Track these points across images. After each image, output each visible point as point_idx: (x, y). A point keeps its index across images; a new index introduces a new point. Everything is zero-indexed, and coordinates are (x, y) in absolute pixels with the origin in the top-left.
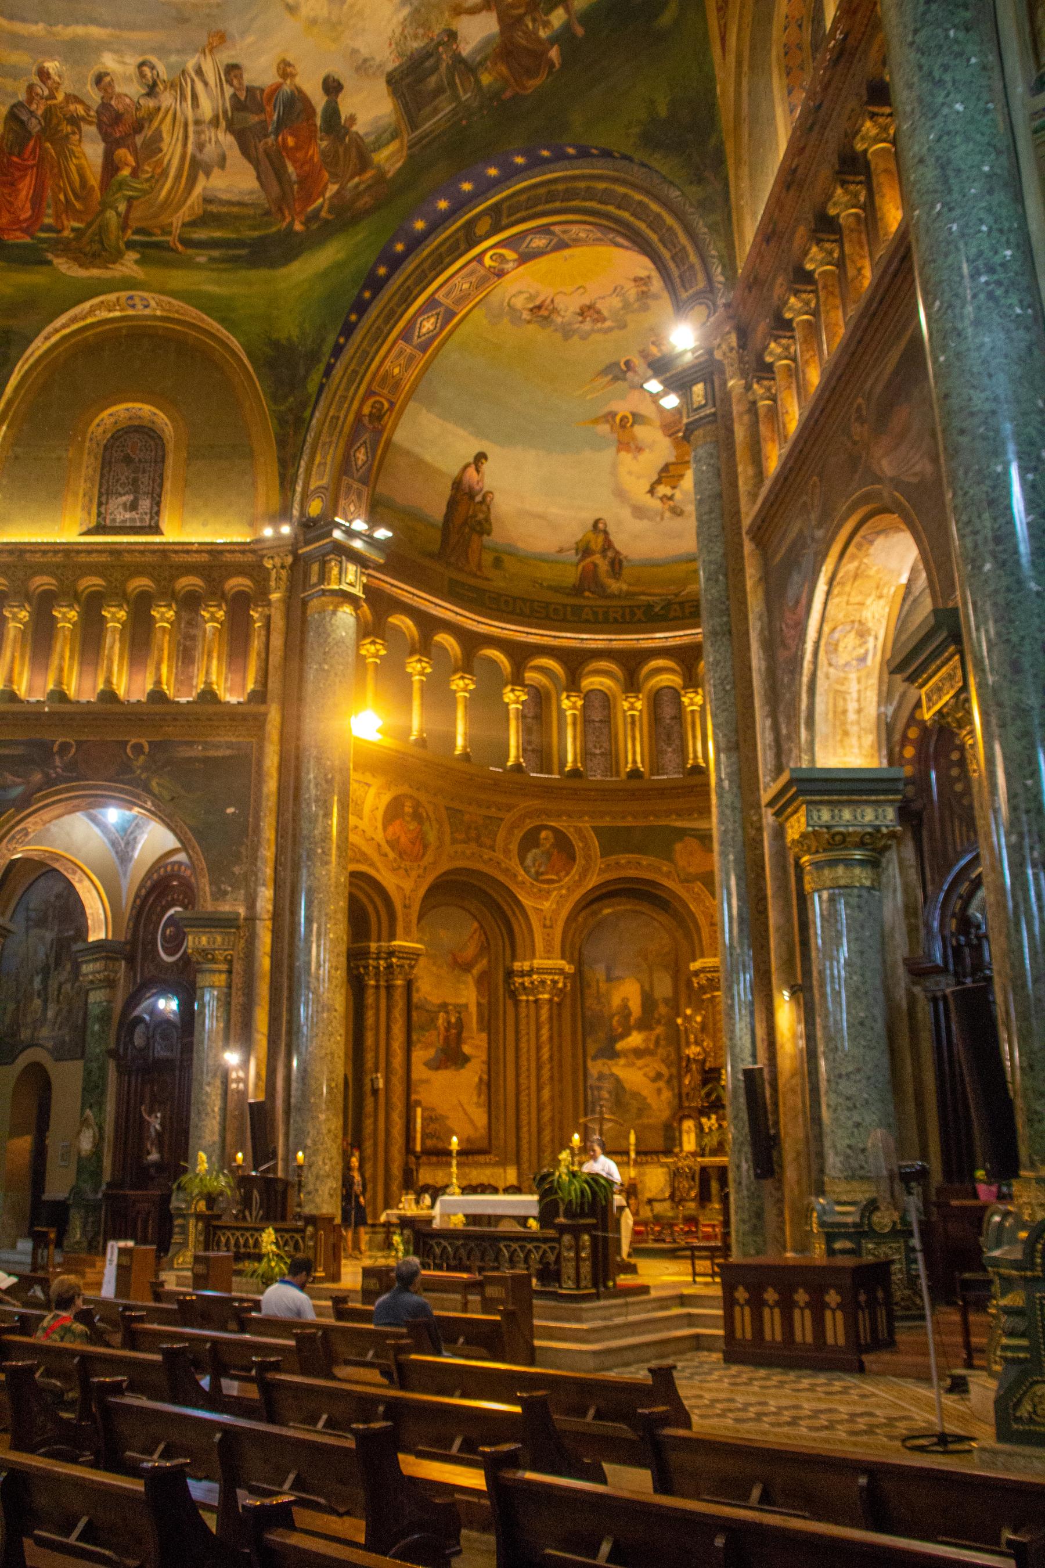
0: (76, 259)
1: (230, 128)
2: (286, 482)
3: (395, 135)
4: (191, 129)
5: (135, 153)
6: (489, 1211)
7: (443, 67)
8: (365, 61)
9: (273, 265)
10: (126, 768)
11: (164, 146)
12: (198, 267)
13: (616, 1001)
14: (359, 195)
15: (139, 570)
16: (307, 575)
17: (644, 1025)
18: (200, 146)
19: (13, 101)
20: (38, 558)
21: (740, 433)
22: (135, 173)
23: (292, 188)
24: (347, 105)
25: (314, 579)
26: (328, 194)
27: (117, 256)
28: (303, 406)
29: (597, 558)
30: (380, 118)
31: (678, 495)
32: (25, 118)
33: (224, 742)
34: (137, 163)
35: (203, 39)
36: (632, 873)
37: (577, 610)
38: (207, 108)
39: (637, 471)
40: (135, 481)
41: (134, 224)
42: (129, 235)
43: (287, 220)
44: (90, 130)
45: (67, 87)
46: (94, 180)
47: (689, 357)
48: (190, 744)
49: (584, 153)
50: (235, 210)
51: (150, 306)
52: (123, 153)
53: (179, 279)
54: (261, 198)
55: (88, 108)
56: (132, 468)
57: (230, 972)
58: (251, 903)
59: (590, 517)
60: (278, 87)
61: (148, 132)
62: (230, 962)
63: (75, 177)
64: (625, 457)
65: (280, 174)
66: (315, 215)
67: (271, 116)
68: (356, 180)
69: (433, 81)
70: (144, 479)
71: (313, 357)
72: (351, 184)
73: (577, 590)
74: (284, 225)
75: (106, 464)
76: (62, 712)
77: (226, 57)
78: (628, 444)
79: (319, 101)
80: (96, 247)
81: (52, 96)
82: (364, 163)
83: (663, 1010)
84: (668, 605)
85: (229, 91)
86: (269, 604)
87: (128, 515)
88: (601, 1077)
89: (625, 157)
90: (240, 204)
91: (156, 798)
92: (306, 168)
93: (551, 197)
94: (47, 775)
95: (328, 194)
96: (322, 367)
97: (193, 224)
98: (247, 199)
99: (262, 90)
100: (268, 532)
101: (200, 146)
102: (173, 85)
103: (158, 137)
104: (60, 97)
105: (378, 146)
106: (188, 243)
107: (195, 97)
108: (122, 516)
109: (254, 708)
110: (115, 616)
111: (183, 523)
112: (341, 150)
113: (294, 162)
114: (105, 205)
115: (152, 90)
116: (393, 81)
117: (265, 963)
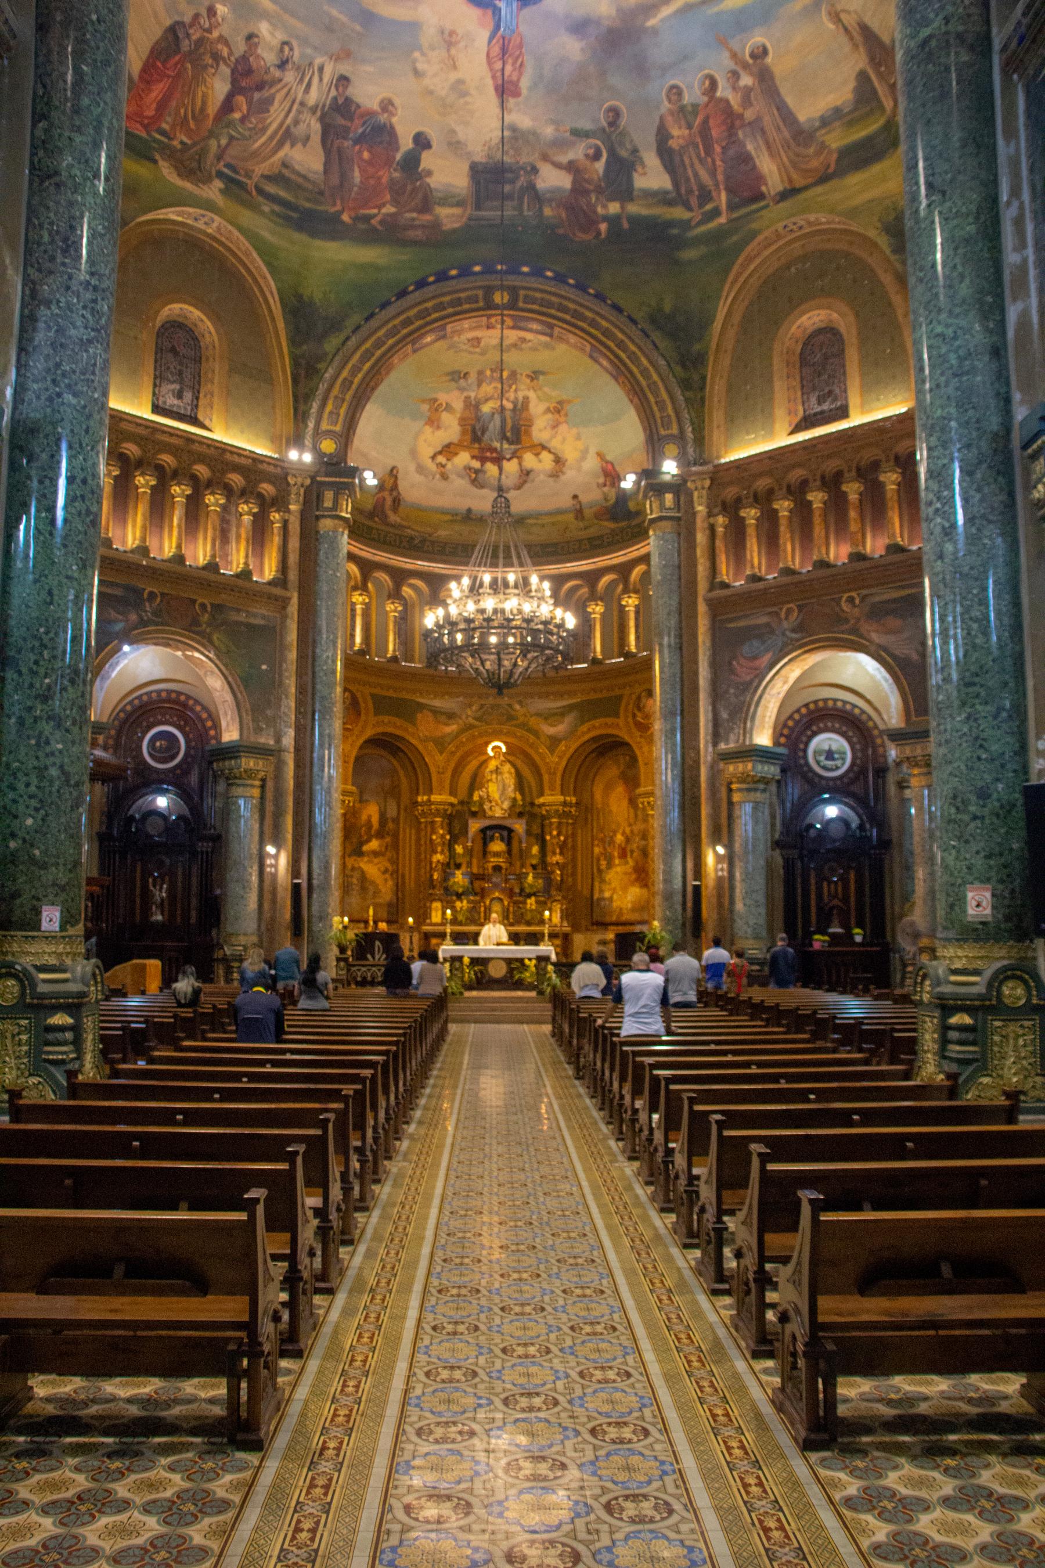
0: (176, 168)
1: (322, 119)
2: (300, 416)
3: (460, 204)
5: (250, 104)
6: (484, 955)
7: (518, 184)
9: (313, 234)
10: (195, 622)
11: (272, 110)
12: (262, 213)
13: (364, 817)
14: (413, 227)
15: (202, 459)
16: (319, 498)
17: (380, 835)
18: (296, 122)
19: (177, 18)
20: (131, 428)
21: (701, 538)
22: (243, 120)
24: (427, 160)
25: (328, 503)
27: (207, 180)
28: (320, 359)
29: (386, 494)
31: (449, 466)
32: (181, 35)
33: (260, 614)
36: (390, 730)
37: (370, 528)
38: (313, 97)
39: (430, 440)
40: (180, 373)
41: (227, 158)
42: (221, 166)
43: (338, 207)
44: (225, 70)
45: (224, 30)
46: (212, 110)
47: (667, 478)
48: (238, 610)
49: (599, 297)
50: (300, 180)
51: (211, 225)
52: (241, 100)
53: (247, 217)
54: (319, 178)
55: (231, 53)
56: (177, 359)
57: (263, 787)
58: (278, 740)
59: (390, 463)
61: (266, 93)
62: (263, 780)
63: (199, 103)
64: (428, 429)
66: (367, 219)
69: (507, 188)
70: (187, 374)
71: (335, 325)
72: (408, 215)
73: (371, 515)
74: (332, 210)
75: (159, 350)
76: (175, 571)
77: (344, 68)
78: (433, 422)
79: (406, 143)
80: (194, 165)
81: (209, 31)
82: (426, 206)
83: (391, 825)
84: (424, 541)
85: (333, 93)
86: (288, 511)
87: (176, 402)
88: (353, 869)
89: (630, 318)
90: (305, 177)
91: (217, 649)
92: (372, 182)
93: (562, 308)
94: (140, 617)
95: (384, 211)
96: (342, 337)
97: (268, 178)
98: (311, 176)
99: (358, 106)
100: (293, 455)
101: (296, 122)
102: (298, 68)
103: (270, 101)
104: (215, 34)
105: (444, 202)
106: (260, 191)
107: (309, 85)
108: (171, 401)
109: (277, 591)
110: (179, 491)
111: (227, 428)
112: (409, 188)
113: (362, 171)
114: (212, 134)
115: (282, 65)
116: (476, 171)
117: (291, 783)
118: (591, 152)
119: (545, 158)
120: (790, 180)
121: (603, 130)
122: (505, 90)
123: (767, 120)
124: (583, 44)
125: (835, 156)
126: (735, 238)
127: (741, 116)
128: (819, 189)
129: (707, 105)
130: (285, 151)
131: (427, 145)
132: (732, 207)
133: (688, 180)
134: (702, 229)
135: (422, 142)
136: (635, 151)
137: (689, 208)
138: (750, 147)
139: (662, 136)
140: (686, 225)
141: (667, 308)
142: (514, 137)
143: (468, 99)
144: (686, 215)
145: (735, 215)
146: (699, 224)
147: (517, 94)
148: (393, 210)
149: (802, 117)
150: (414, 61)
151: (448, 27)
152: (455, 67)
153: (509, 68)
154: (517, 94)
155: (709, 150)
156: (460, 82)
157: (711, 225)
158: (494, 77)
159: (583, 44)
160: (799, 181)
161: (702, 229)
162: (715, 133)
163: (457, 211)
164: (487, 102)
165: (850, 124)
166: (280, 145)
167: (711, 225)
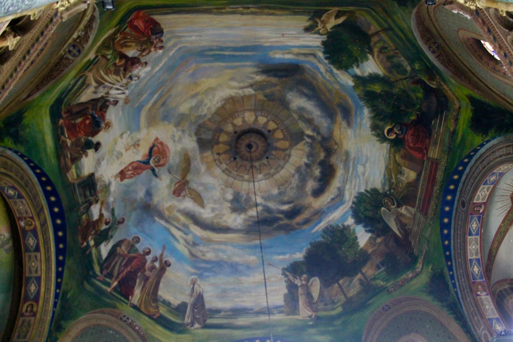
1: (103, 97)
4: (111, 85)
8: (100, 163)
18: (104, 87)
23: (73, 119)
26: (68, 140)
30: (84, 169)
34: (117, 66)
35: (131, 98)
60: (104, 120)
65: (79, 114)
66: (63, 133)
67: (97, 113)
68: (69, 156)
69: (88, 193)
77: (121, 103)
79: (95, 139)
85: (112, 100)
95: (68, 140)
99: (105, 112)
105: (77, 168)
107: (118, 89)
113: (81, 123)
114: (114, 50)
116: (92, 176)
118: (108, 220)
119: (102, 203)
120: (140, 305)
121: (116, 220)
122: (122, 175)
123: (151, 280)
124: (143, 197)
125: (158, 315)
126: (108, 300)
127: (145, 271)
128: (147, 318)
129: (140, 255)
130: (94, 84)
131: (96, 149)
132: (115, 289)
133: (110, 264)
134: (99, 284)
135: (97, 146)
136: (112, 237)
137: (101, 273)
138: (138, 281)
139: (119, 244)
140: (95, 276)
141: (69, 295)
142: (107, 187)
143: (116, 160)
144: (98, 272)
145: (114, 293)
146: (99, 280)
147: (122, 180)
148: (69, 145)
149: (160, 293)
150: (126, 132)
151: (141, 143)
152: (127, 150)
153: (130, 172)
154: (122, 180)
155: (126, 265)
156: (122, 154)
157: (104, 287)
158: (126, 168)
159: (143, 197)
160: (143, 308)
161: (99, 284)
162: (134, 263)
163: (75, 177)
164: (116, 168)
165: (170, 312)
166: (97, 81)
167: (104, 287)
